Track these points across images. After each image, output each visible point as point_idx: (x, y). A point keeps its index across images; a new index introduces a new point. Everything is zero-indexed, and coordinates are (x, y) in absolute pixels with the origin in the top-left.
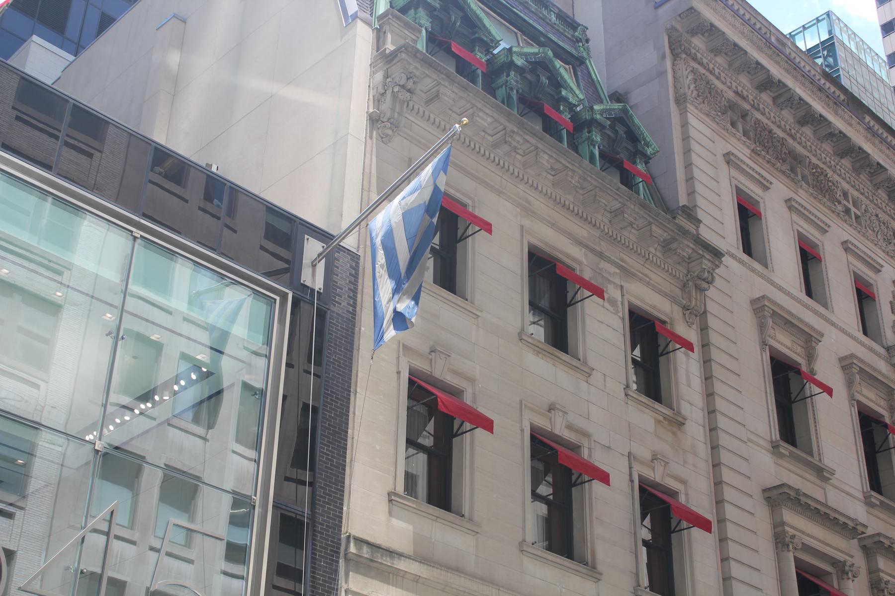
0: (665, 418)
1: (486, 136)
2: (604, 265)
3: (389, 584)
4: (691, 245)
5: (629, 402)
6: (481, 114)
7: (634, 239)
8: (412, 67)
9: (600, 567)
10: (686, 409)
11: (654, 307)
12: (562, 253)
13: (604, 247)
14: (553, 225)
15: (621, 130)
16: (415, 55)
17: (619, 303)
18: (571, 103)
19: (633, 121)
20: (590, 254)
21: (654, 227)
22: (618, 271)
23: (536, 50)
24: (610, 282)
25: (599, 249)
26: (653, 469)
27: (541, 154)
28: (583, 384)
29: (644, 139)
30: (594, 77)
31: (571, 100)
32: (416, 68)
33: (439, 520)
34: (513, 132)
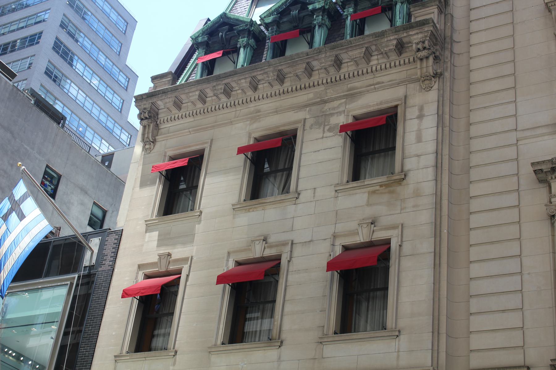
0: (381, 186)
4: (392, 38)
5: (339, 195)
6: (191, 94)
9: (283, 336)
10: (410, 164)
11: (381, 103)
12: (284, 125)
13: (331, 93)
14: (277, 112)
18: (319, 9)
20: (314, 108)
21: (350, 53)
22: (344, 100)
24: (332, 115)
25: (319, 100)
27: (239, 82)
28: (291, 209)
34: (214, 86)
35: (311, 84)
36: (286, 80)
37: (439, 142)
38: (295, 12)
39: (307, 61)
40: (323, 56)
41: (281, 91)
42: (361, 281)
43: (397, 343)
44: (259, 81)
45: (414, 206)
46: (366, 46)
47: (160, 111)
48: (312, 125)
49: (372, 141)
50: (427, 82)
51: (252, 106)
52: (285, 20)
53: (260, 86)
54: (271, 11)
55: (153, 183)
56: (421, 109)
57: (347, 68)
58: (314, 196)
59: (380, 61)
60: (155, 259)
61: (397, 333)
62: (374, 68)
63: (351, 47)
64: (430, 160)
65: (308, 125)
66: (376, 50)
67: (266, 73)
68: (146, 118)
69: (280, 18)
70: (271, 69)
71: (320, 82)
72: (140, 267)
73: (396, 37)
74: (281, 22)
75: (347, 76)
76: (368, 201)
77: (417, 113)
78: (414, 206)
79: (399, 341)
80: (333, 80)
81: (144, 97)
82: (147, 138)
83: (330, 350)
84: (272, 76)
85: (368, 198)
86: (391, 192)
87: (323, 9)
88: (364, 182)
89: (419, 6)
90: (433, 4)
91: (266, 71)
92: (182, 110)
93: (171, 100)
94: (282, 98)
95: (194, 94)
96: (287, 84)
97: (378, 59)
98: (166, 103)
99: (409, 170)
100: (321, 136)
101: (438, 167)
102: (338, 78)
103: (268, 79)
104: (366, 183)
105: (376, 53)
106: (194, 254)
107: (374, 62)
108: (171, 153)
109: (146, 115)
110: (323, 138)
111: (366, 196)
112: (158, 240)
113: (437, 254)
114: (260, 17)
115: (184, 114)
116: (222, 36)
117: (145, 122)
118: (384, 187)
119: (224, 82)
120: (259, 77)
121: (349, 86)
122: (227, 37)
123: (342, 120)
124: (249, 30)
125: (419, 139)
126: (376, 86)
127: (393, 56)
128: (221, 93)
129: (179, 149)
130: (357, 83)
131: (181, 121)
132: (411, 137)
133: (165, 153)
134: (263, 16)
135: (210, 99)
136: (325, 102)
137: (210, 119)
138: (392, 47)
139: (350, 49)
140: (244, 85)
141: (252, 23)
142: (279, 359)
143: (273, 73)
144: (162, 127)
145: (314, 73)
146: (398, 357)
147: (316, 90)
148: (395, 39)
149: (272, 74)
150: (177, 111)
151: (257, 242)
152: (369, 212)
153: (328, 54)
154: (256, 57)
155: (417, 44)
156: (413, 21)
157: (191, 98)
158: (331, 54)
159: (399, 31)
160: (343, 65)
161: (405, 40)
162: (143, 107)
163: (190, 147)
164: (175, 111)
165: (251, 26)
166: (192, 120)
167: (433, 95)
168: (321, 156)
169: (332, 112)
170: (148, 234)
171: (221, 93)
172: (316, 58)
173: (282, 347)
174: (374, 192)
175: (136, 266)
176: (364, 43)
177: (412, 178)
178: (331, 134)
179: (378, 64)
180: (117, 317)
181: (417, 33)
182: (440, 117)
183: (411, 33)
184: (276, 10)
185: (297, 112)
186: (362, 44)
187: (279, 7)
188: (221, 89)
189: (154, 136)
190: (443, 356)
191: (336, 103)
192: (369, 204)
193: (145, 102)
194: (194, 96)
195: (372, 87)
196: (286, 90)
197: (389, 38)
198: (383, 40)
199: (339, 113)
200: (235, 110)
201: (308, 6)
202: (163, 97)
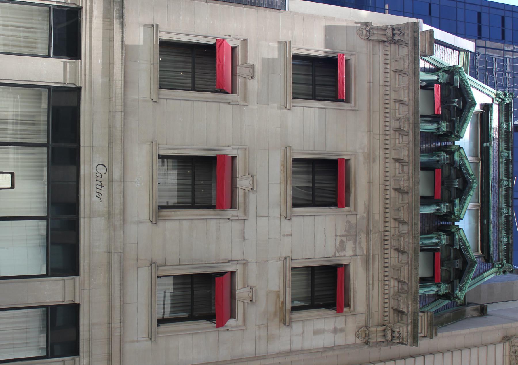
0: (282, 303)
1: (397, 111)
2: (363, 236)
3: (104, 18)
4: (410, 309)
5: (282, 262)
6: (406, 91)
7: (392, 263)
8: (407, 31)
9: (161, 224)
10: (297, 328)
11: (355, 292)
13: (375, 237)
14: (370, 182)
15: (458, 264)
16: (414, 32)
17: (343, 254)
18: (453, 210)
19: (470, 273)
20: (365, 221)
21: (406, 267)
22: (365, 252)
23: (471, 173)
24: (355, 242)
25: (371, 228)
26: (244, 288)
27: (407, 148)
28: (276, 212)
29: (463, 286)
30: (485, 274)
31: (456, 209)
32: (408, 34)
33: (152, 66)
34: (408, 120)
35: (387, 220)
36: (397, 193)
39: (410, 224)
40: (410, 241)
41: (388, 188)
42: (203, 297)
43: (145, 339)
44: (403, 166)
45: (260, 337)
46: (409, 284)
47: (397, 46)
48: (350, 222)
49: (323, 287)
50: (364, 335)
51: (379, 153)
52: (452, 172)
53: (397, 164)
54: (464, 159)
55: (328, 44)
56: (342, 330)
57: (393, 257)
58: (284, 235)
59: (392, 289)
60: (250, 61)
61: (153, 339)
62: (387, 283)
63: (412, 268)
64: (297, 346)
65: (350, 218)
66: (403, 289)
67: (409, 179)
68: (394, 35)
69: (455, 168)
70: (411, 185)
71: (387, 229)
72: (245, 41)
73: (410, 313)
74: (451, 167)
75: (386, 256)
76: (271, 292)
77: (339, 326)
78: (260, 337)
79: (146, 341)
80: (386, 242)
81: (416, 34)
82: (373, 33)
83: (144, 273)
84: (404, 185)
85: (274, 292)
86: (275, 314)
87: (452, 212)
88: (289, 287)
89: (430, 320)
90: (429, 334)
91: (411, 180)
92: (392, 73)
93: (406, 67)
94: (381, 186)
95: (406, 95)
96: (393, 194)
97: (394, 287)
98: (404, 61)
99: (291, 327)
100: (337, 234)
102: (386, 247)
103: (403, 180)
104: (288, 289)
105: (400, 286)
106: (250, 107)
107: (392, 283)
108: (352, 62)
109: (397, 37)
110: (336, 236)
111: (276, 289)
112: (269, 59)
114: (462, 148)
115: (388, 75)
116: (454, 102)
117: (389, 33)
118: (281, 305)
119: (410, 132)
120: (406, 168)
121: (377, 256)
122: (452, 107)
124: (452, 133)
126: (371, 285)
127: (393, 303)
128: (400, 126)
129: (355, 71)
130: (377, 266)
131: (382, 70)
132: (319, 324)
133: (355, 55)
134: (462, 150)
135: (397, 108)
136: (368, 233)
137: (377, 104)
138: (401, 307)
139: (410, 268)
140: (403, 154)
142: (140, 222)
143: (407, 186)
144: (380, 46)
145: (397, 223)
146: (133, 342)
147: (380, 222)
148: (408, 312)
149: (406, 184)
150: (393, 68)
151: (251, 182)
152: (262, 294)
153: (411, 245)
154: (426, 137)
155: (399, 332)
156: (420, 314)
157: (403, 90)
158: (410, 249)
159: (414, 315)
160: (397, 253)
161: (404, 317)
162: (406, 31)
163: (355, 84)
164: (394, 66)
165: (455, 136)
166: (381, 84)
167: (351, 339)
168: (319, 235)
169: (358, 242)
170: (276, 45)
171: (400, 126)
172: (410, 233)
173: (150, 223)
174: (278, 297)
175: (246, 38)
176: (412, 282)
177: (285, 333)
178: (338, 244)
179: (390, 287)
181: (408, 333)
183: (409, 326)
184: (464, 164)
185: (365, 204)
186: (412, 280)
187: (466, 167)
188: (404, 127)
189: (374, 41)
191: (364, 245)
192: (269, 292)
193: (409, 36)
194: (404, 94)
195: (371, 282)
196: (388, 192)
197: (410, 306)
198: (410, 300)
199: (355, 250)
200: (381, 133)
201: (458, 199)
202: (410, 59)
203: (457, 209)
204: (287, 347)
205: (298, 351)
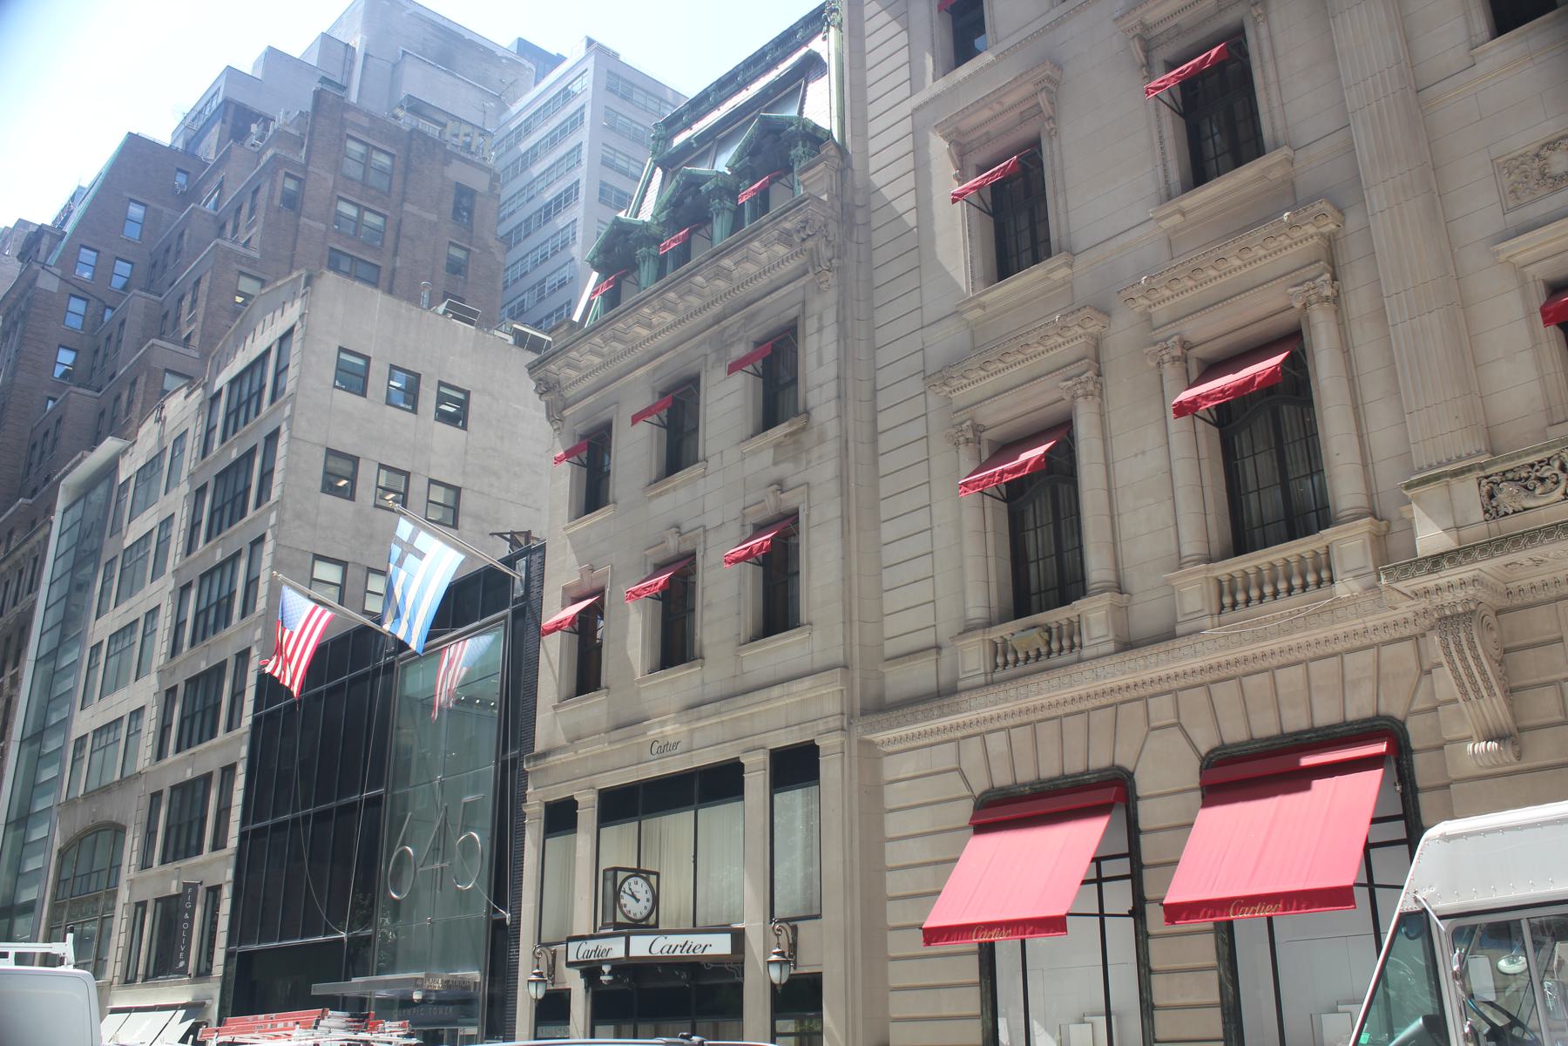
24: (732, 344)
37: (843, 359)
38: (689, 200)
45: (820, 457)
56: (820, 318)
64: (830, 390)
87: (717, 188)
101: (840, 397)
113: (845, 519)
123: (739, 351)
125: (820, 363)
141: (646, 225)
152: (776, 473)
180: (553, 655)
182: (841, 322)
190: (856, 650)
203: (710, 185)
204: (833, 403)
205: (839, 386)
